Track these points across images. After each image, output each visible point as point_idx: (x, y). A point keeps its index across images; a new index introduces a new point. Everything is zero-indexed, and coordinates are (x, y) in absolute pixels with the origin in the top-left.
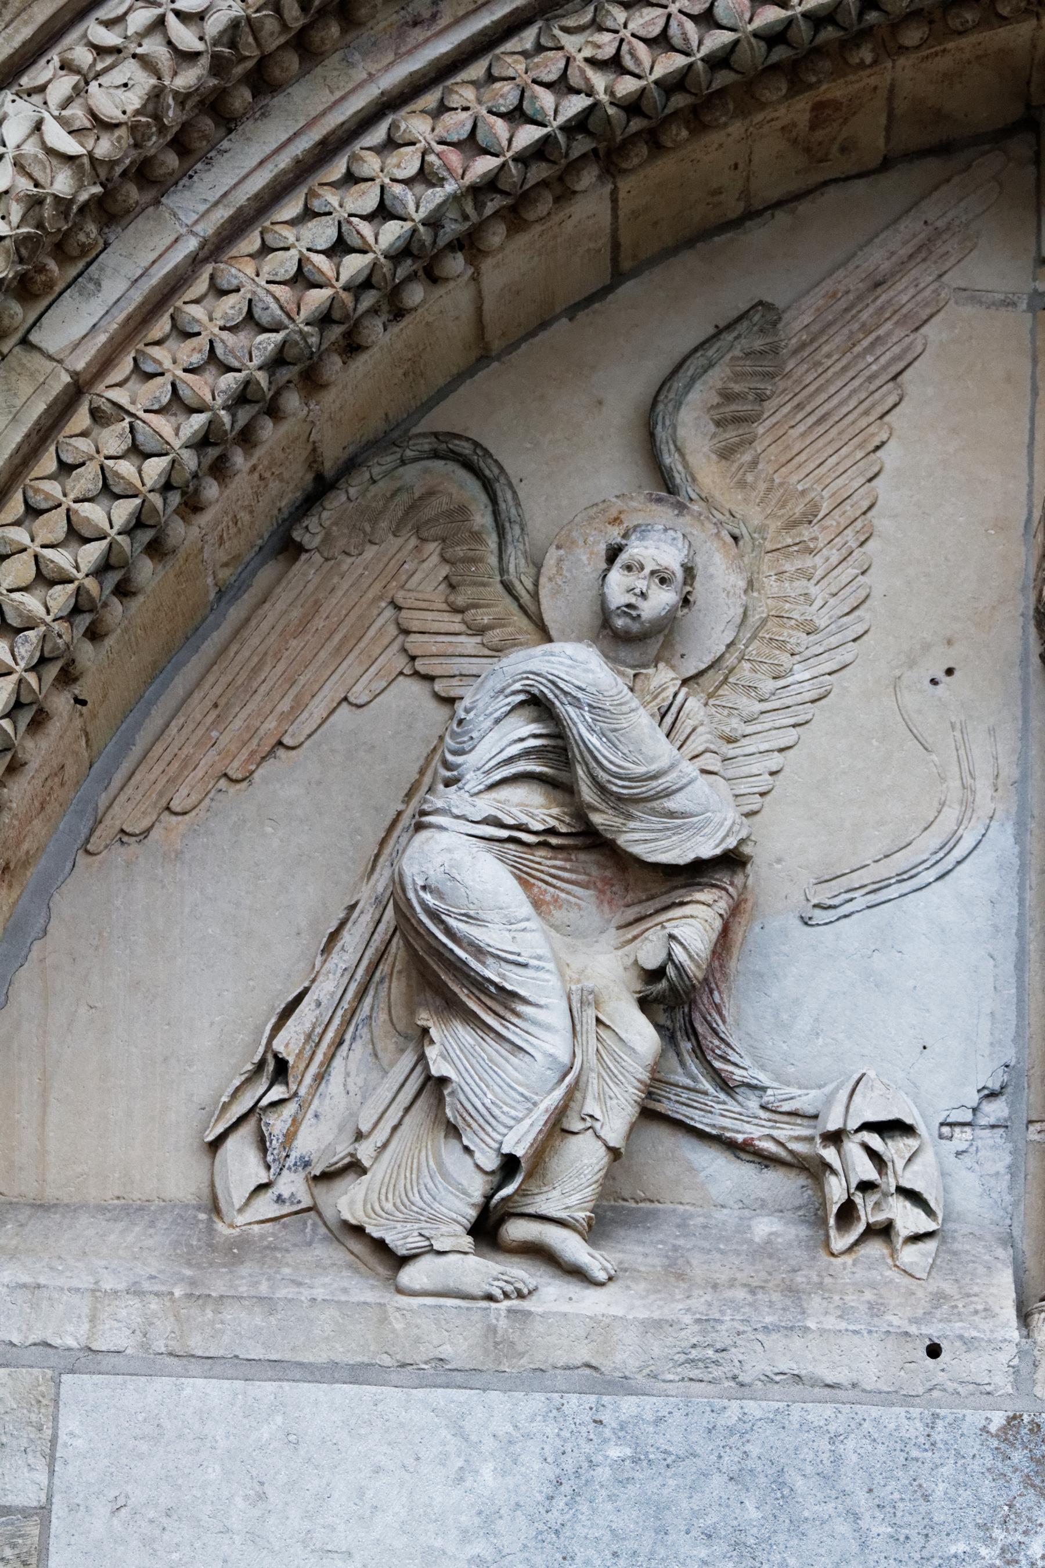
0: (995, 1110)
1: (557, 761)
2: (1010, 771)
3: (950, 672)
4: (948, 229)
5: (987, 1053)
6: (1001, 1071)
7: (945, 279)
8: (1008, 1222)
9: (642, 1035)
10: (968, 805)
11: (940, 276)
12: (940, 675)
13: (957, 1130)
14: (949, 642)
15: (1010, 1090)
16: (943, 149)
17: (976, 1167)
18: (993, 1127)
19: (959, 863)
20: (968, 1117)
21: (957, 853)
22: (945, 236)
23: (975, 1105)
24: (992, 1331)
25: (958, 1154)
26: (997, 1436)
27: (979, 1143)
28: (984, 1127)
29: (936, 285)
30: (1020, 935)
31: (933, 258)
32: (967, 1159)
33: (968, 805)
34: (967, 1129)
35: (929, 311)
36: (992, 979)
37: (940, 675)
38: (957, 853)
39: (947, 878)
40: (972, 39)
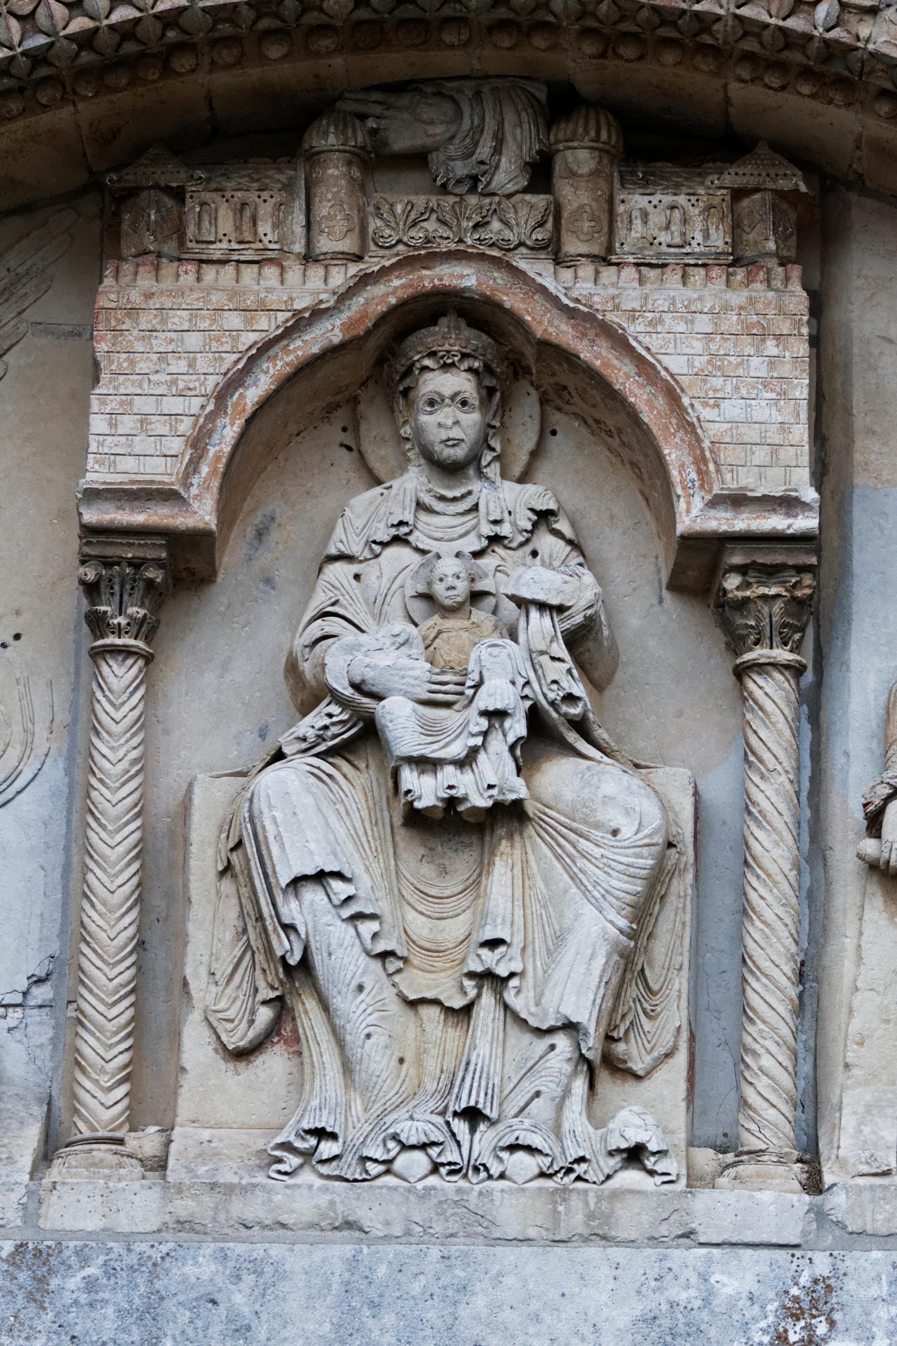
0: (42, 993)
2: (63, 717)
3: (17, 637)
4: (27, 274)
5: (36, 946)
6: (47, 962)
7: (24, 315)
8: (49, 1084)
10: (28, 746)
11: (20, 313)
12: (9, 640)
13: (10, 1010)
14: (18, 613)
15: (54, 976)
16: (26, 209)
17: (25, 1040)
18: (40, 1007)
19: (19, 792)
20: (19, 999)
21: (18, 785)
22: (24, 280)
23: (24, 989)
24: (7, 1176)
25: (10, 1030)
26: (7, 1261)
27: (29, 1020)
28: (33, 1007)
29: (16, 320)
30: (67, 849)
31: (14, 299)
32: (18, 1034)
33: (28, 746)
34: (18, 1009)
35: (9, 343)
36: (42, 887)
37: (9, 640)
38: (18, 785)
39: (9, 805)
40: (20, 124)
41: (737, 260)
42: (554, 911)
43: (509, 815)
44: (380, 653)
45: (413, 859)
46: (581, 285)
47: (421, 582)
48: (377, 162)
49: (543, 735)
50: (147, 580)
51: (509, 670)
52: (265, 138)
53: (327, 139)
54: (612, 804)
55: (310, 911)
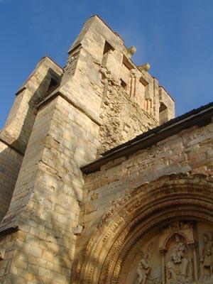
1: (142, 265)
9: (146, 276)
41: (190, 228)
42: (183, 269)
43: (180, 262)
44: (174, 255)
45: (177, 266)
46: (182, 231)
47: (176, 251)
48: (172, 226)
49: (182, 258)
50: (164, 252)
51: (180, 254)
52: (166, 227)
53: (170, 226)
54: (185, 261)
55: (171, 270)
